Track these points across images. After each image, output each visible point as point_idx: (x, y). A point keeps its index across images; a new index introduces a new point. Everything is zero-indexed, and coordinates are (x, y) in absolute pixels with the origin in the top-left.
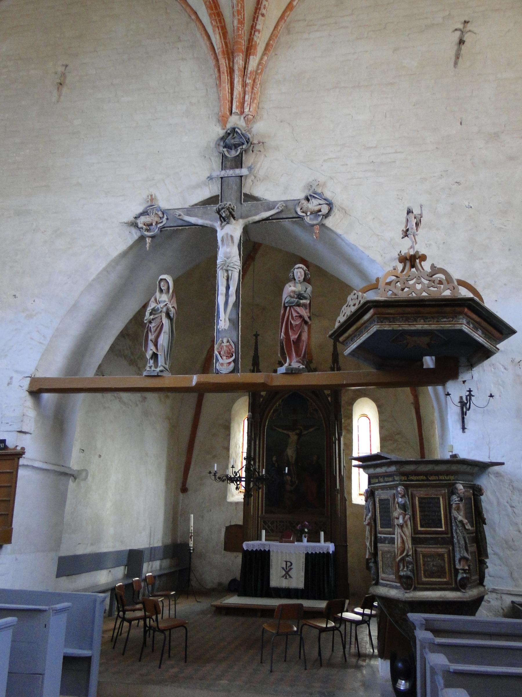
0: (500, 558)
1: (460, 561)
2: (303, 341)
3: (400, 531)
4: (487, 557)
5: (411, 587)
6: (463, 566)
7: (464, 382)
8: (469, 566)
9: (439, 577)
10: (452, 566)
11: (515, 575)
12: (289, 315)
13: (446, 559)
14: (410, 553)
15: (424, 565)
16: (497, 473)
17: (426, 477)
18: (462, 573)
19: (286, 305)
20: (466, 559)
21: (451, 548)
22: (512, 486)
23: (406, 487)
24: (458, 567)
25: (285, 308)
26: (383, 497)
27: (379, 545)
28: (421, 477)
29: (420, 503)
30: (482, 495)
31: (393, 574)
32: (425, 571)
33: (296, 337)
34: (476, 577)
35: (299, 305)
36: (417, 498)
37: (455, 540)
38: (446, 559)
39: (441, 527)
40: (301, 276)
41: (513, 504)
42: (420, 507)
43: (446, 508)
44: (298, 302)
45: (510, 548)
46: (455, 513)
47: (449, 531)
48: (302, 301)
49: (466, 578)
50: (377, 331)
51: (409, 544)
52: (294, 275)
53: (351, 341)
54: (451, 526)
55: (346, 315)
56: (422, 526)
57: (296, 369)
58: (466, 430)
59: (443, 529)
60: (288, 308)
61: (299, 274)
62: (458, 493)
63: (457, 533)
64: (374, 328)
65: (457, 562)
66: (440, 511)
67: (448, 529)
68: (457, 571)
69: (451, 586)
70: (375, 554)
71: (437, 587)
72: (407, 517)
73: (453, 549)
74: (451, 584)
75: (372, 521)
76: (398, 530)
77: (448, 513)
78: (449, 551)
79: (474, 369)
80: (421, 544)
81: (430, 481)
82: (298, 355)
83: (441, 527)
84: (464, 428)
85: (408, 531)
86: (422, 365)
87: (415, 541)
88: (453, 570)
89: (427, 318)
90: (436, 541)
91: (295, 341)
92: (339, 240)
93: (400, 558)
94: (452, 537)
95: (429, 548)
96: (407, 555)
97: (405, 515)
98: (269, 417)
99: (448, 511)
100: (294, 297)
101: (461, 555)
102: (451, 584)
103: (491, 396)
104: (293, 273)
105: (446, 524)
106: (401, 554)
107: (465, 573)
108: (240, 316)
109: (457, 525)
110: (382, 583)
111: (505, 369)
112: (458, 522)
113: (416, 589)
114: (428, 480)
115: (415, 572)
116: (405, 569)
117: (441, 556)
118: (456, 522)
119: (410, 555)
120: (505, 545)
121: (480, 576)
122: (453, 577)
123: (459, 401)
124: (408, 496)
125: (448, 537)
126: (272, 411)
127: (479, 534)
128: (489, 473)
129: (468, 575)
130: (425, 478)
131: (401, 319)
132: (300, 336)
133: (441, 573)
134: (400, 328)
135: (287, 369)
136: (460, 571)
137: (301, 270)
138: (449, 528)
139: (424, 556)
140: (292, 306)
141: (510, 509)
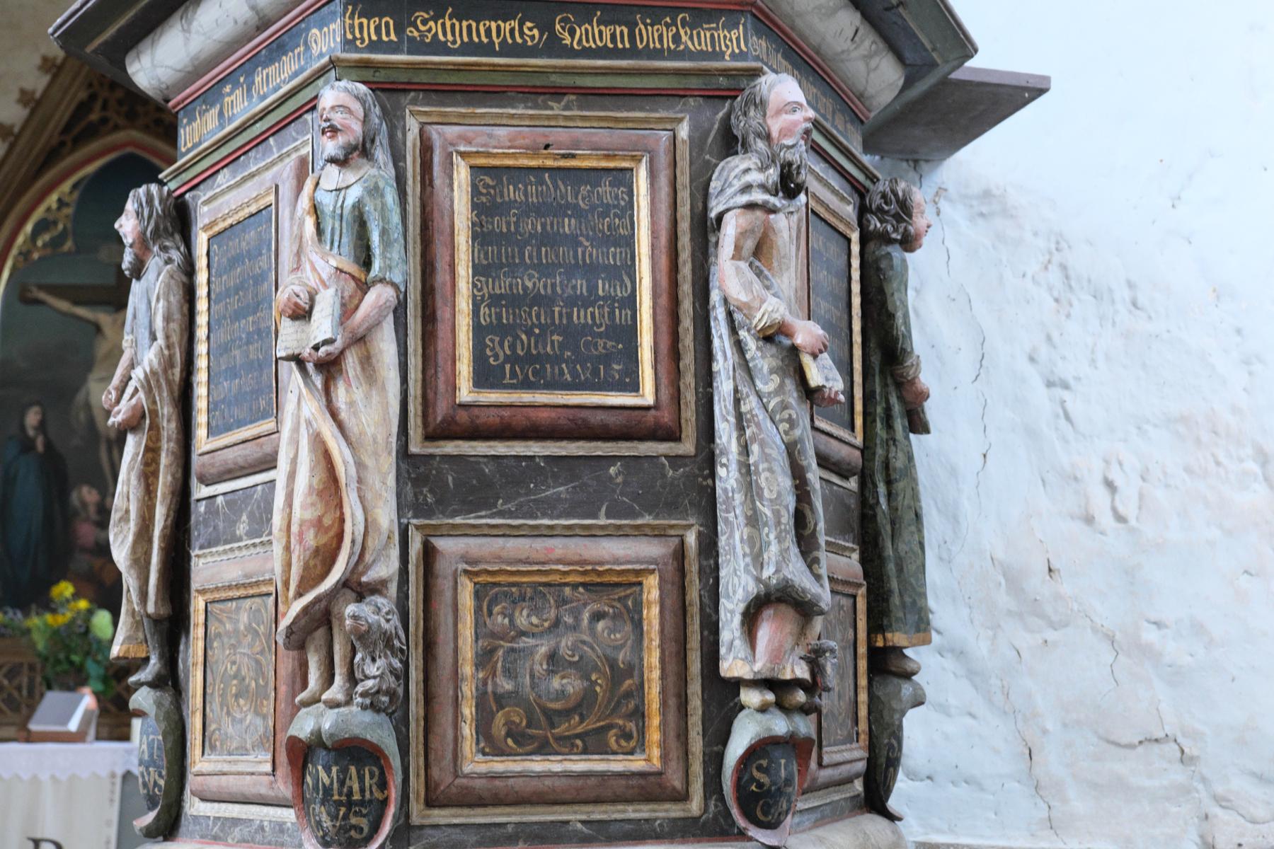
0: (974, 675)
1: (751, 618)
3: (312, 407)
4: (922, 627)
5: (375, 828)
6: (777, 656)
8: (814, 660)
9: (594, 744)
10: (695, 666)
11: (1052, 762)
13: (652, 615)
14: (385, 568)
15: (484, 659)
16: (987, 195)
17: (546, 27)
18: (763, 709)
20: (804, 609)
21: (691, 539)
22: (1063, 267)
23: (390, 89)
24: (733, 665)
29: (483, 208)
30: (909, 243)
32: (487, 705)
34: (848, 756)
36: (462, 174)
37: (727, 477)
38: (652, 615)
41: (1065, 370)
42: (480, 236)
43: (674, 284)
45: (1030, 609)
46: (731, 277)
47: (689, 414)
49: (797, 747)
51: (375, 506)
54: (707, 377)
56: (483, 378)
62: (767, 137)
63: (741, 422)
65: (730, 628)
66: (630, 268)
67: (677, 397)
68: (724, 694)
69: (674, 811)
72: (379, 296)
73: (709, 546)
74: (682, 797)
76: (299, 400)
77: (686, 288)
78: (680, 554)
80: (471, 507)
81: (570, 53)
83: (634, 387)
85: (373, 406)
88: (695, 688)
90: (587, 492)
93: (297, 606)
94: (708, 458)
95: (537, 533)
96: (355, 587)
98: (14, 251)
99: (686, 270)
101: (768, 572)
102: (682, 797)
105: (671, 353)
106: (307, 582)
107: (782, 707)
109: (745, 365)
112: (751, 345)
114: (553, 47)
115: (416, 709)
116: (336, 691)
117: (615, 589)
118: (739, 346)
119: (377, 588)
120: (1004, 600)
121: (872, 747)
122: (697, 744)
124: (397, 157)
125: (675, 460)
126: (29, 228)
127: (882, 489)
128: (941, 191)
129: (805, 726)
130: (532, 32)
136: (751, 697)
138: (689, 397)
139: (494, 591)
141: (1041, 398)
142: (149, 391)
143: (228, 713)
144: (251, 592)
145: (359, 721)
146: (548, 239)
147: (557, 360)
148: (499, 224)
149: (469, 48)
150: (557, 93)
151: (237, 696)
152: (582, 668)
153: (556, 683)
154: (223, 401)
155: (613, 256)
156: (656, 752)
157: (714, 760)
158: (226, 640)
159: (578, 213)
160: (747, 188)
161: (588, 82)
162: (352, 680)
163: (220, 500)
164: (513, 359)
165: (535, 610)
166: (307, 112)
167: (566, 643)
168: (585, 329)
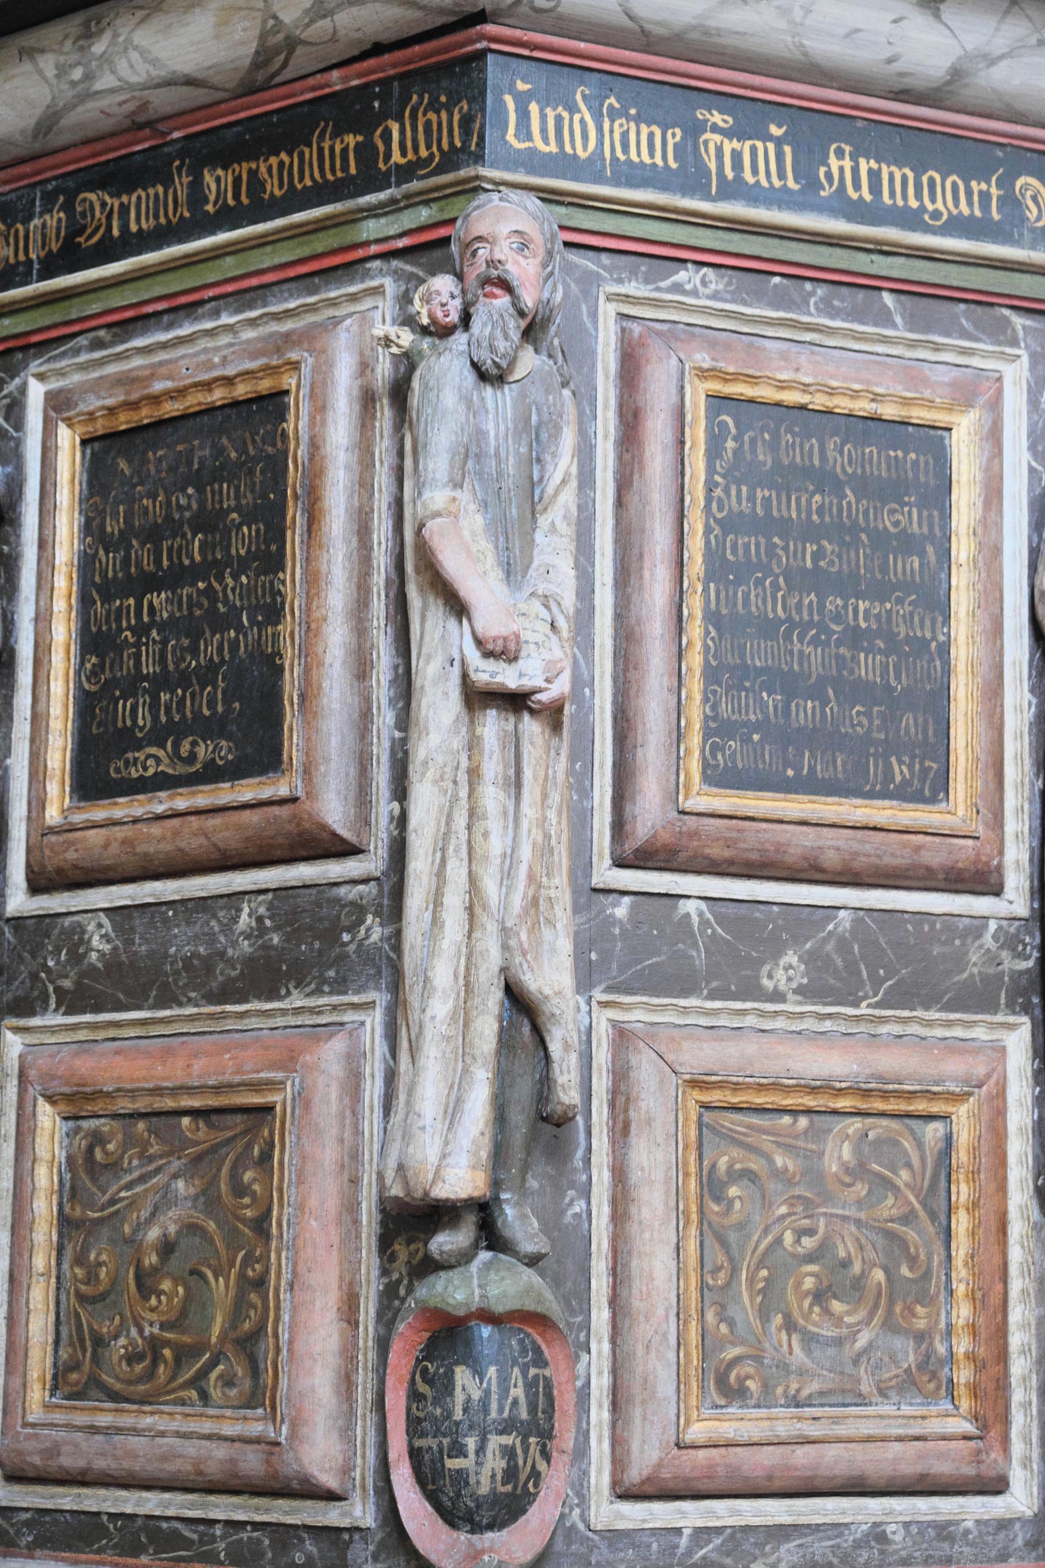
31: (928, 1378)
110: (614, 1536)
143: (790, 1326)
144: (880, 1105)
154: (757, 727)
158: (772, 1186)
163: (690, 907)
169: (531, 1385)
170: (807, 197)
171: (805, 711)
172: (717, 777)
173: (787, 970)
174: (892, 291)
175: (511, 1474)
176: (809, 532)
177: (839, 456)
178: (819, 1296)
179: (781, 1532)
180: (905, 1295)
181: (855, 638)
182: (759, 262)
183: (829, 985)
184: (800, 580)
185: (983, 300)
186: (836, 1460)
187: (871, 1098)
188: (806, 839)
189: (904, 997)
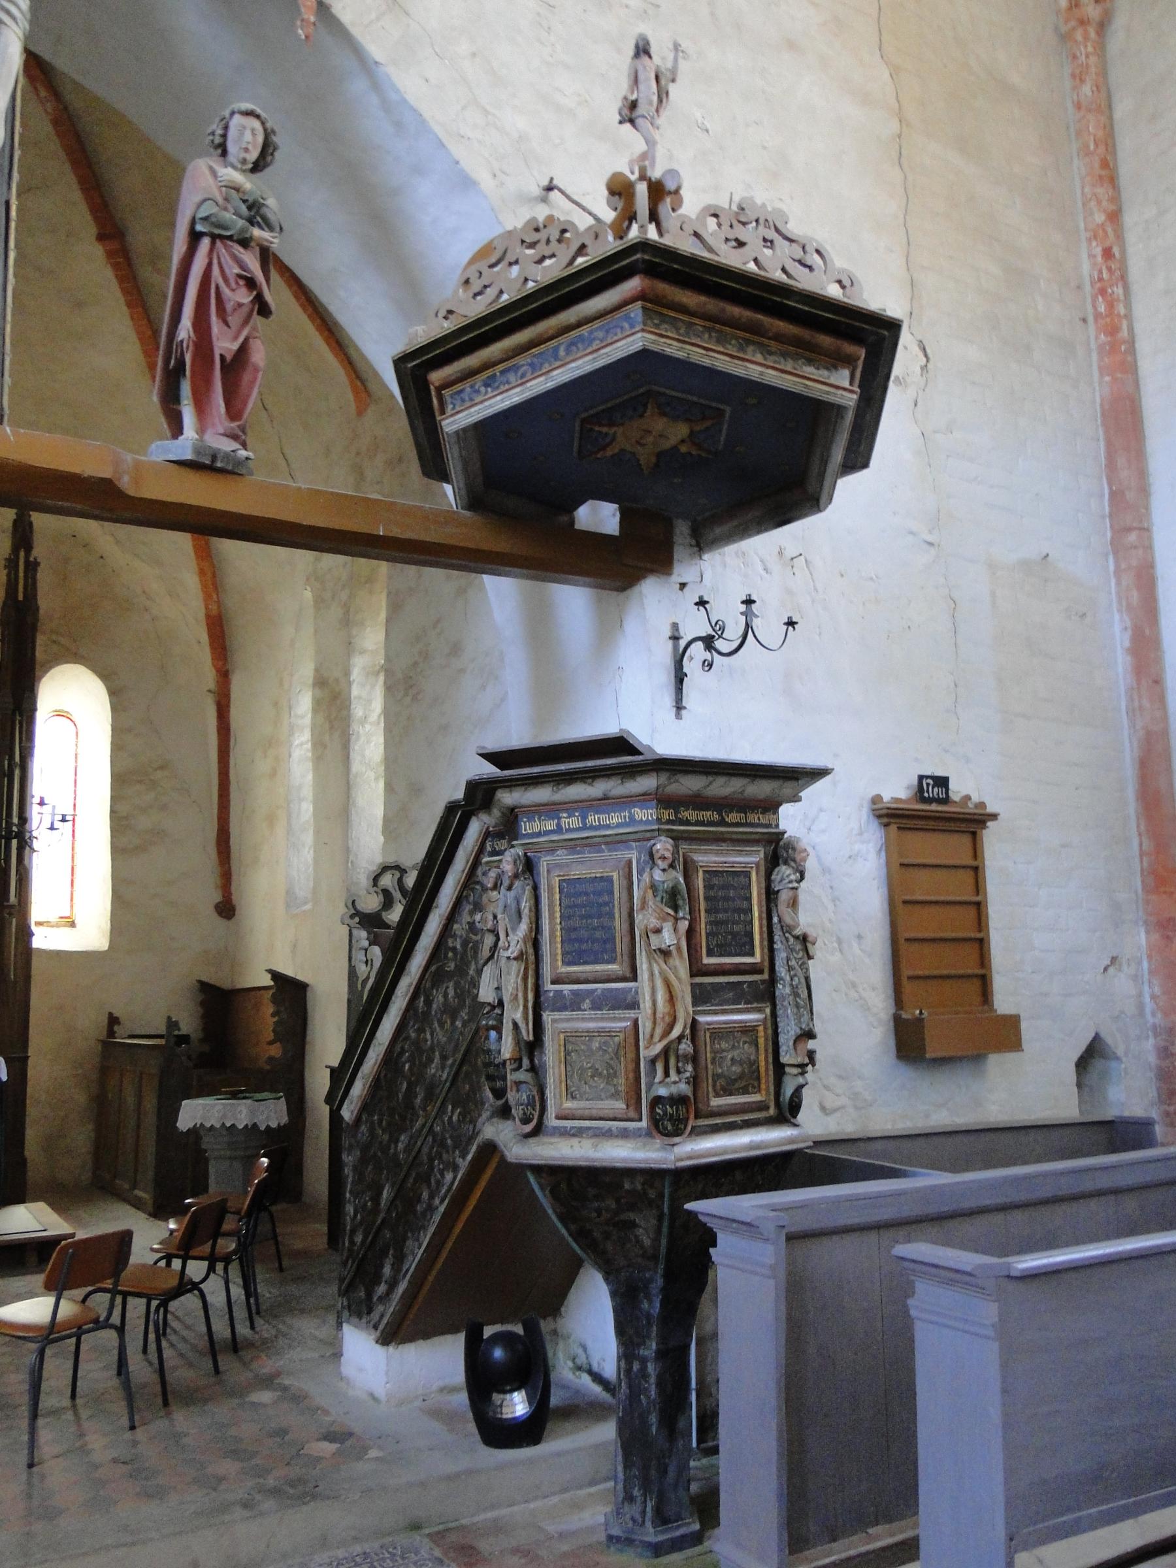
2: (256, 370)
7: (683, 586)
9: (745, 1091)
12: (209, 266)
15: (713, 1060)
17: (720, 814)
19: (199, 228)
23: (676, 838)
24: (785, 1059)
25: (195, 237)
26: (584, 867)
27: (547, 1017)
28: (708, 815)
29: (708, 887)
31: (615, 1096)
33: (235, 346)
35: (245, 243)
36: (701, 874)
37: (783, 990)
39: (752, 954)
40: (255, 146)
44: (243, 230)
48: (256, 232)
50: (644, 355)
52: (224, 136)
53: (486, 385)
55: (491, 293)
57: (227, 456)
58: (683, 712)
59: (757, 958)
60: (206, 242)
61: (248, 136)
62: (794, 861)
64: (630, 340)
70: (533, 1047)
71: (737, 1118)
75: (530, 945)
79: (706, 557)
82: (234, 412)
83: (752, 954)
84: (679, 707)
86: (572, 522)
87: (701, 996)
89: (771, 353)
91: (229, 358)
92: (358, 85)
94: (773, 980)
96: (680, 1038)
97: (676, 919)
100: (225, 209)
102: (767, 1108)
103: (791, 623)
104: (226, 128)
108: (13, 213)
110: (555, 1128)
111: (766, 569)
113: (698, 1132)
123: (669, 634)
125: (763, 982)
131: (707, 336)
132: (243, 350)
133: (747, 1080)
134: (706, 362)
135: (197, 451)
137: (256, 124)
140: (221, 237)
142: (525, 943)
145: (684, 1088)
146: (726, 899)
147: (730, 945)
148: (712, 893)
149: (701, 823)
150: (724, 840)
151: (592, 1077)
152: (741, 1063)
153: (734, 1068)
155: (745, 905)
156: (763, 1092)
157: (778, 1094)
159: (735, 888)
160: (791, 882)
161: (734, 836)
162: (679, 1072)
164: (717, 945)
165: (727, 1042)
166: (634, 841)
167: (736, 1053)
168: (738, 933)
169: (528, 1097)
170: (585, 828)
171: (584, 947)
172: (566, 963)
173: (587, 1004)
174: (607, 843)
175: (524, 1114)
176: (584, 906)
177: (589, 888)
178: (592, 1077)
179: (589, 1128)
180: (611, 1077)
181: (595, 929)
182: (573, 846)
183: (596, 1006)
184: (582, 917)
185: (626, 842)
186: (594, 1113)
187: (600, 1032)
188: (584, 975)
189: (613, 1008)
